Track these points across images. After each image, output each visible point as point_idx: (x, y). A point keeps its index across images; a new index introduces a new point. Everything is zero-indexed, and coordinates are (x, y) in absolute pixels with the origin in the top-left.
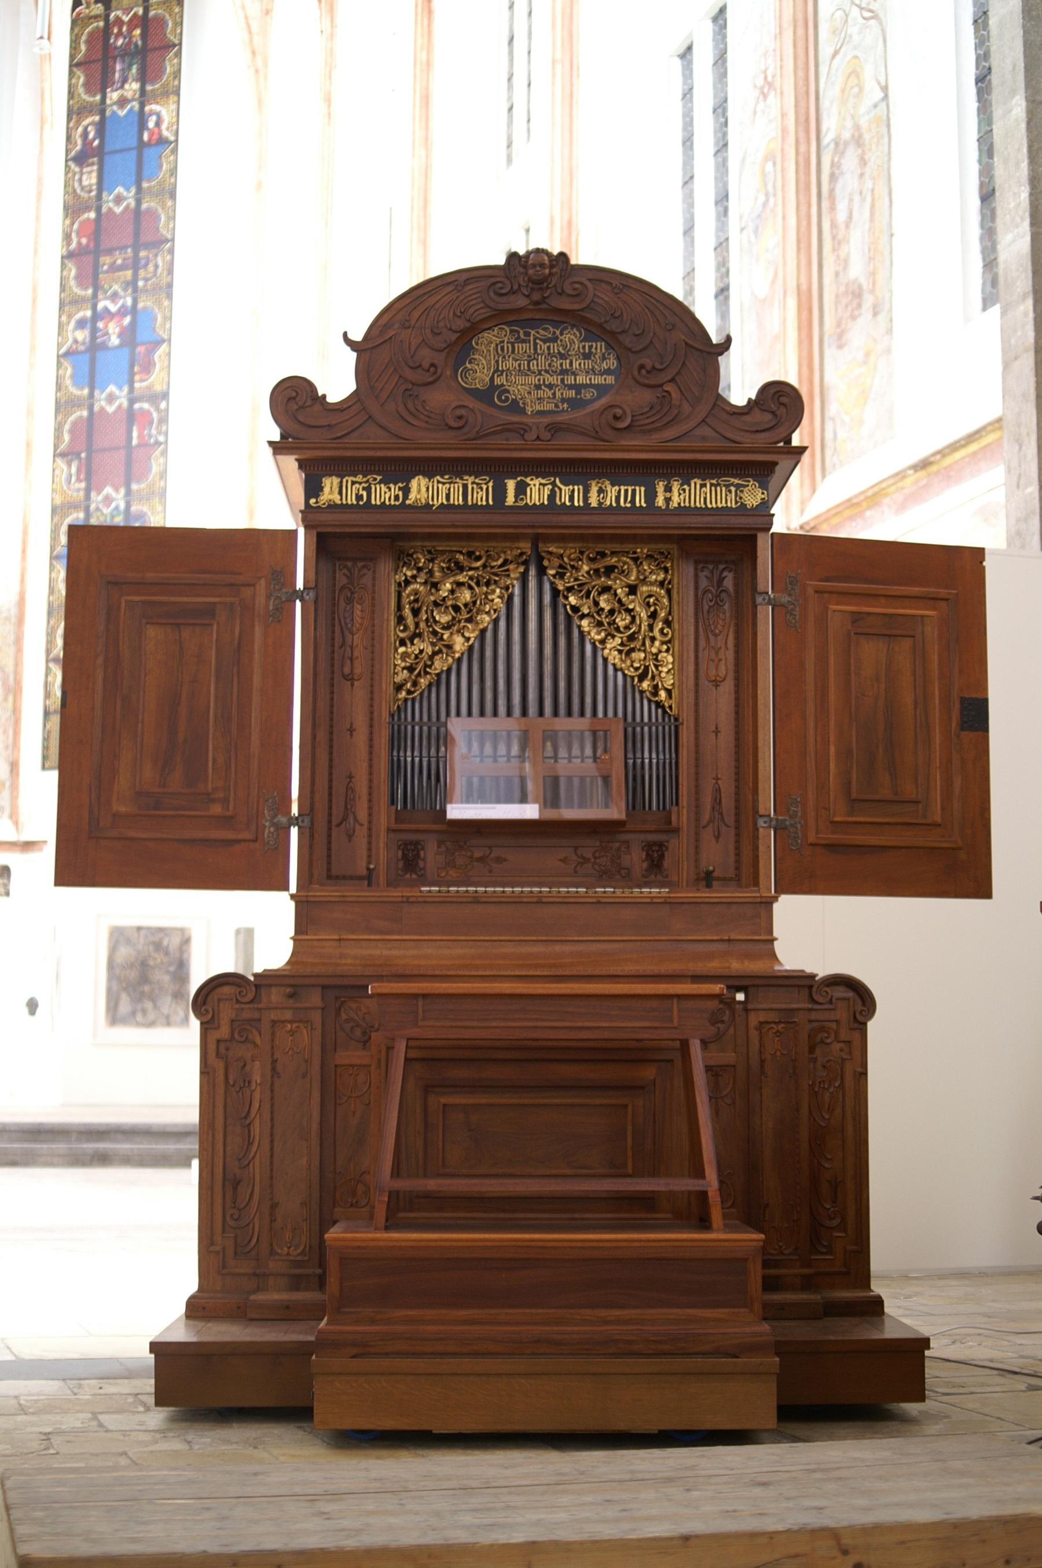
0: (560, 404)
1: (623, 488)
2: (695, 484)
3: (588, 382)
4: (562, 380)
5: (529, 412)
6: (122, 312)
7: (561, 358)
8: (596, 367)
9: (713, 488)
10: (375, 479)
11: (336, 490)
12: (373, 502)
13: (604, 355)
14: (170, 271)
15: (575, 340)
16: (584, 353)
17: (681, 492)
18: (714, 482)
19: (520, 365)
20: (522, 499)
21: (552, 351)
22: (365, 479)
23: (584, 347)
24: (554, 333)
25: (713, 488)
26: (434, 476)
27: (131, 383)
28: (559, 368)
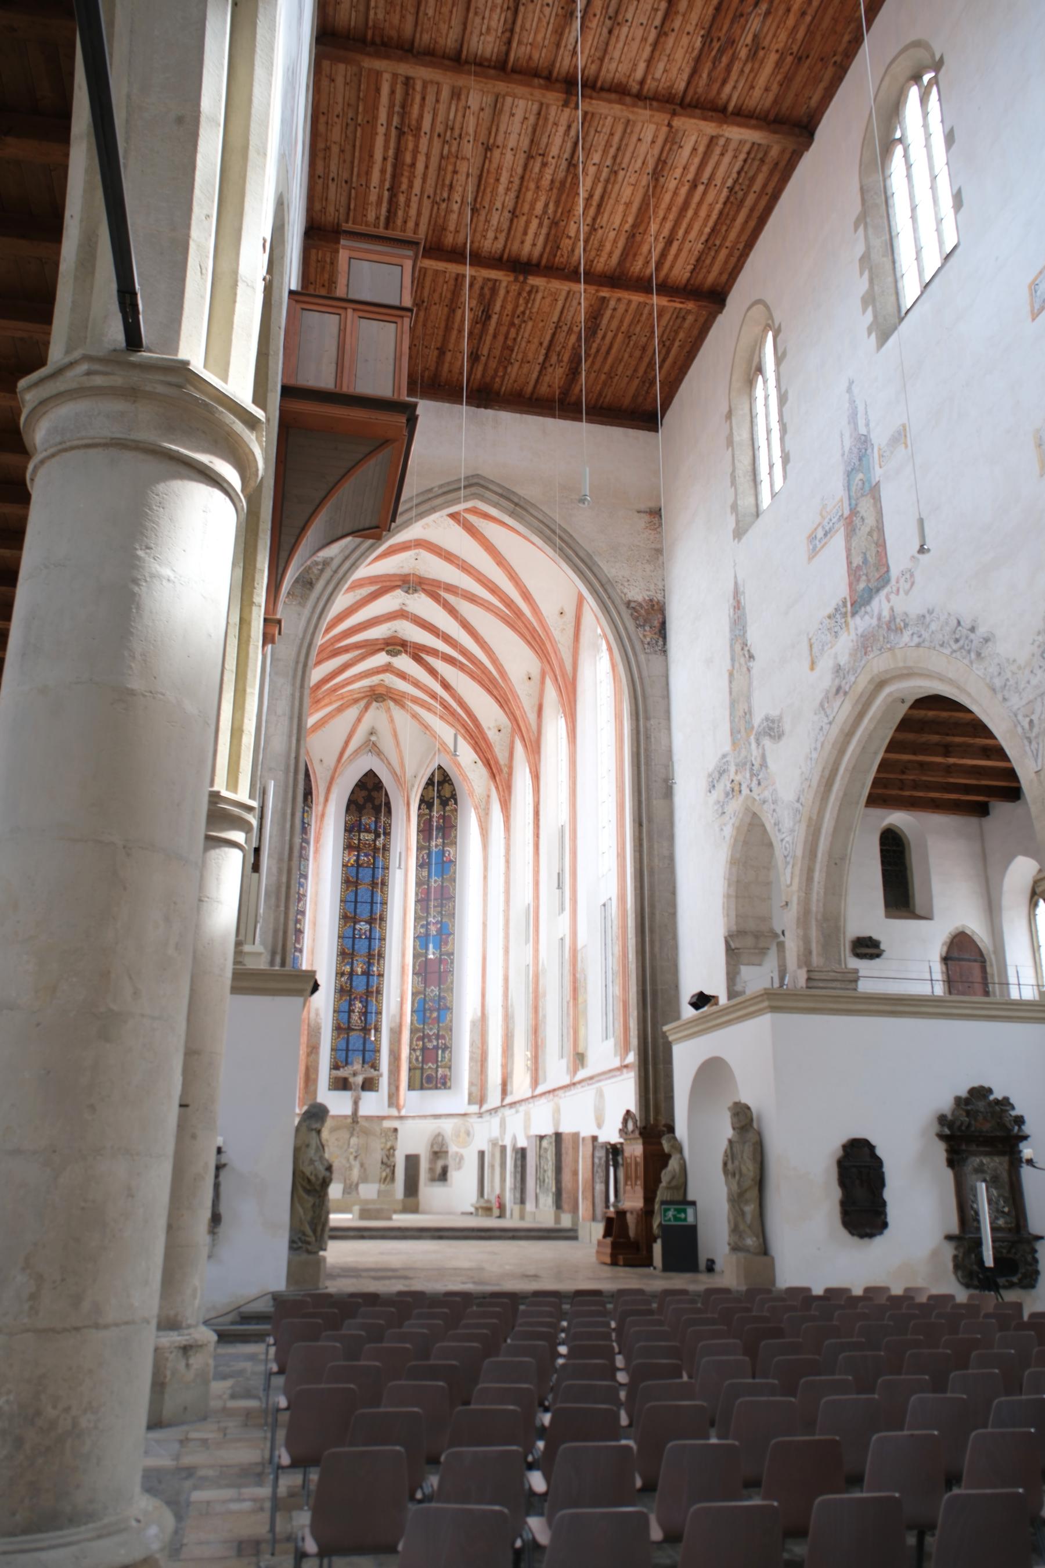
6: (437, 923)
14: (454, 909)
27: (440, 948)
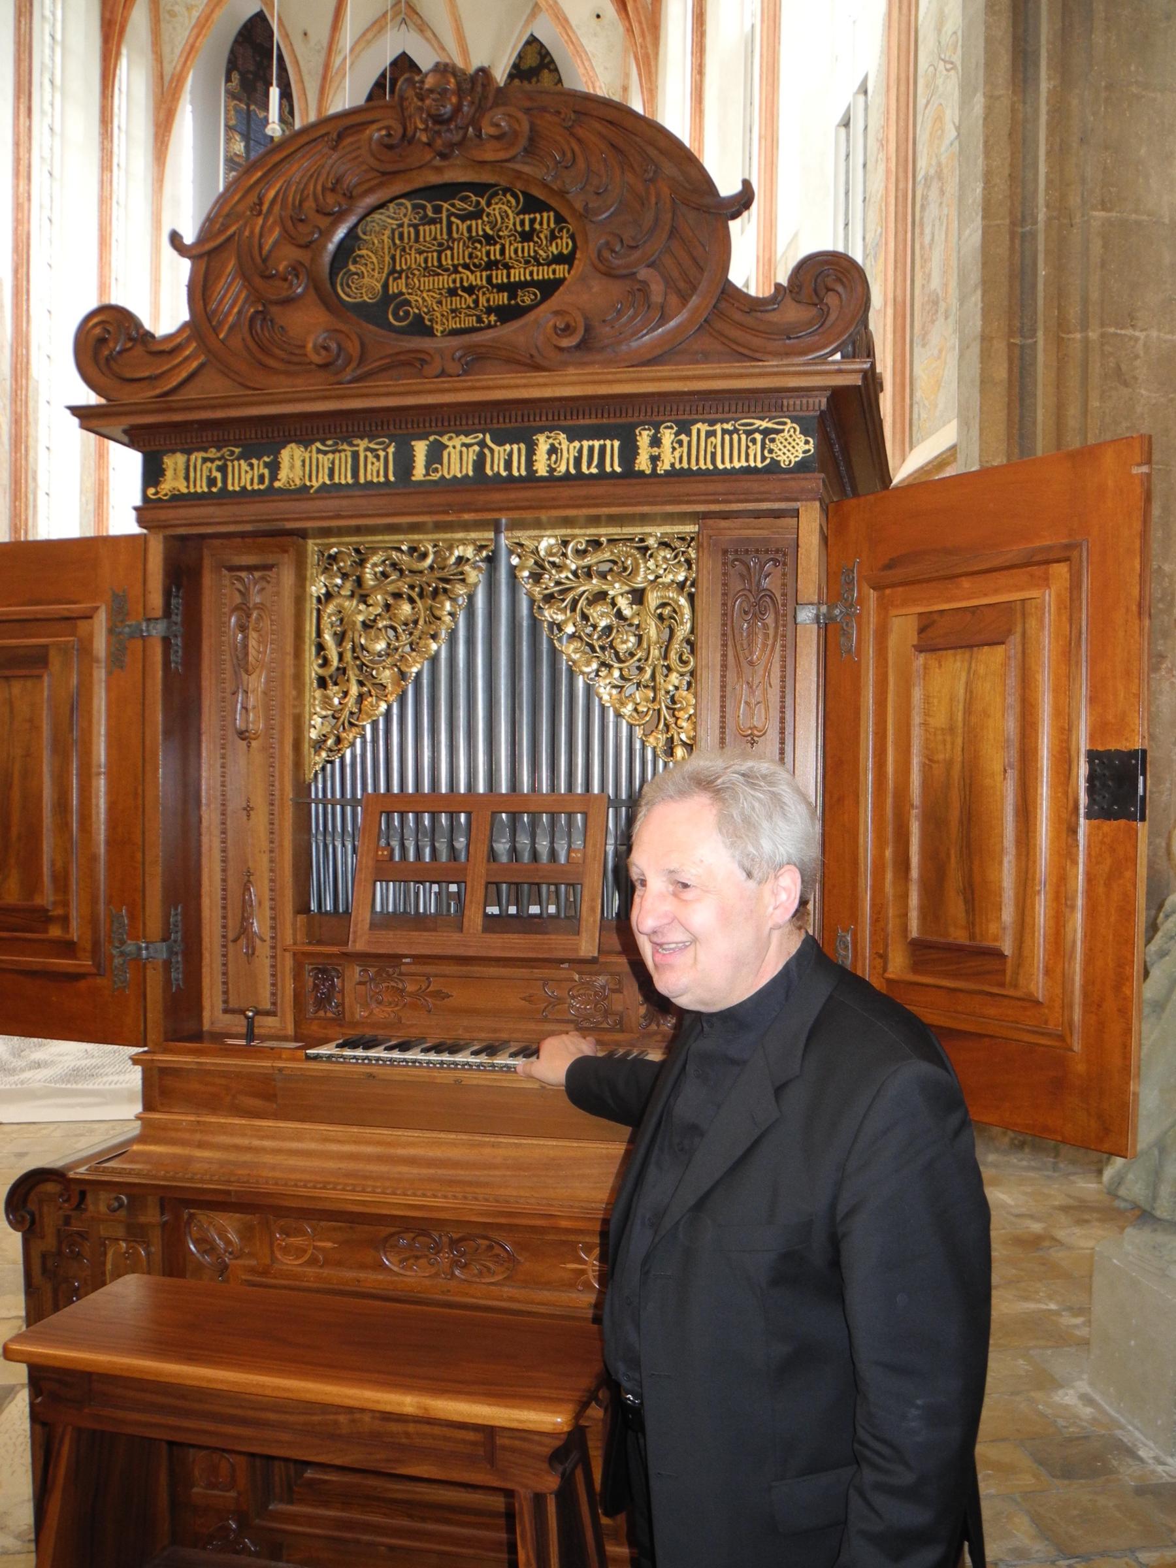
0: (484, 317)
1: (586, 444)
2: (699, 431)
3: (528, 278)
4: (489, 279)
5: (438, 328)
7: (489, 244)
8: (541, 252)
9: (727, 437)
10: (232, 453)
11: (182, 474)
12: (230, 488)
13: (552, 232)
15: (509, 212)
16: (524, 230)
17: (676, 446)
18: (729, 426)
19: (426, 260)
20: (436, 470)
21: (474, 234)
22: (219, 455)
23: (522, 223)
24: (478, 203)
25: (727, 437)
26: (313, 442)
28: (485, 259)
